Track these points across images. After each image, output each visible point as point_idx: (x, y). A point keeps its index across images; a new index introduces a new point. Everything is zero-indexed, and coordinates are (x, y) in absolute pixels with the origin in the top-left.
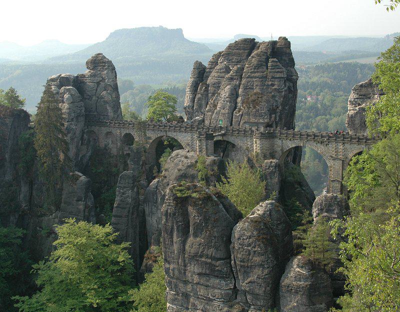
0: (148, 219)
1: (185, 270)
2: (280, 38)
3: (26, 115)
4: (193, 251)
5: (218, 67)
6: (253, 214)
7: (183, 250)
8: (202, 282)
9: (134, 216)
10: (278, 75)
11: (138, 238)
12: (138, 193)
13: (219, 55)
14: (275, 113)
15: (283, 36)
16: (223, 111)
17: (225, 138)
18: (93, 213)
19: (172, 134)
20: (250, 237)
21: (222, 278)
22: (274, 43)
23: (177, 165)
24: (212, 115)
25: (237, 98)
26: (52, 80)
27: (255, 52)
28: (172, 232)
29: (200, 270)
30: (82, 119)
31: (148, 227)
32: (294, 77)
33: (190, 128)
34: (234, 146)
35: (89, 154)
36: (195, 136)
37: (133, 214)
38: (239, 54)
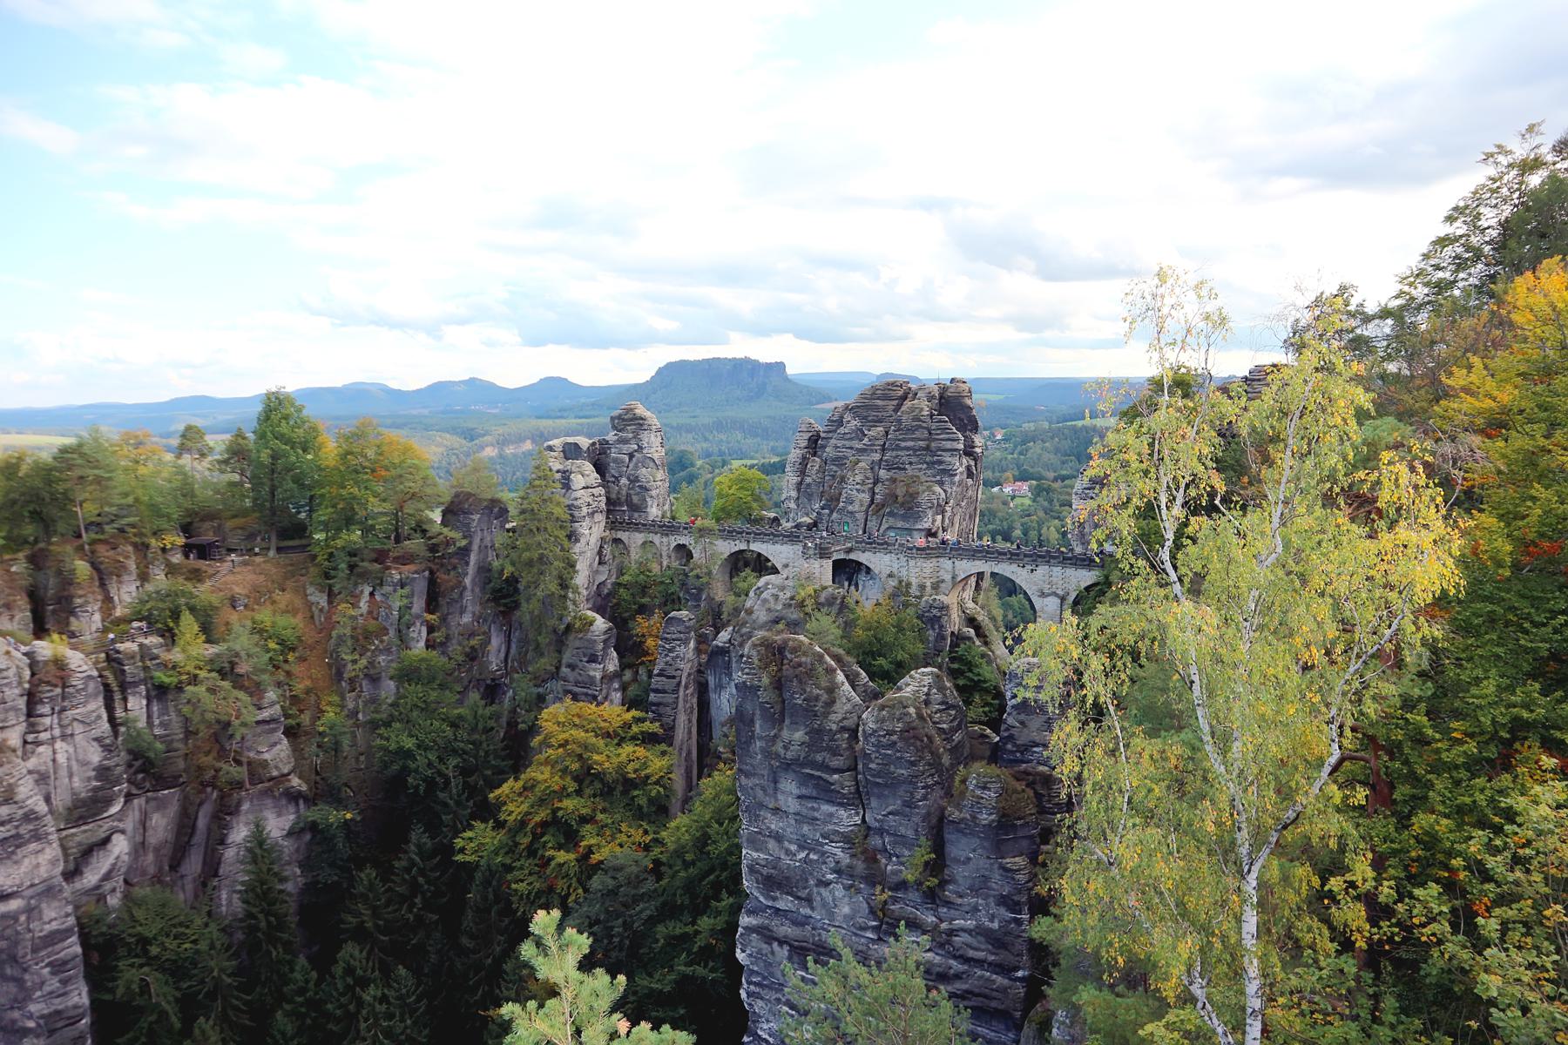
0: (713, 696)
1: (776, 789)
2: (952, 380)
3: (503, 513)
4: (789, 755)
5: (842, 430)
6: (900, 689)
7: (768, 754)
8: (804, 812)
9: (689, 691)
10: (948, 445)
11: (694, 730)
12: (698, 651)
13: (847, 408)
14: (943, 512)
15: (958, 376)
16: (850, 508)
17: (852, 556)
18: (616, 685)
19: (757, 547)
20: (890, 733)
21: (841, 805)
22: (943, 389)
23: (765, 601)
24: (830, 515)
25: (875, 484)
26: (550, 448)
27: (908, 404)
28: (752, 721)
29: (804, 791)
30: (600, 518)
31: (713, 712)
32: (978, 450)
33: (791, 537)
34: (868, 570)
35: (613, 579)
36: (799, 547)
37: (686, 687)
38: (884, 408)
